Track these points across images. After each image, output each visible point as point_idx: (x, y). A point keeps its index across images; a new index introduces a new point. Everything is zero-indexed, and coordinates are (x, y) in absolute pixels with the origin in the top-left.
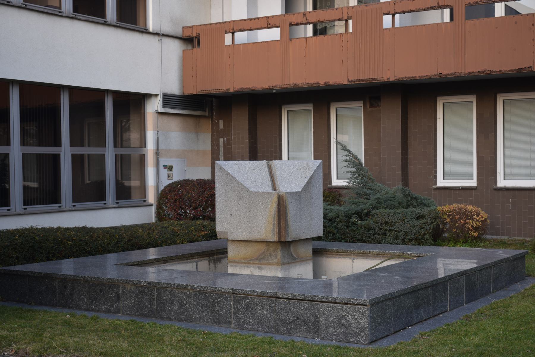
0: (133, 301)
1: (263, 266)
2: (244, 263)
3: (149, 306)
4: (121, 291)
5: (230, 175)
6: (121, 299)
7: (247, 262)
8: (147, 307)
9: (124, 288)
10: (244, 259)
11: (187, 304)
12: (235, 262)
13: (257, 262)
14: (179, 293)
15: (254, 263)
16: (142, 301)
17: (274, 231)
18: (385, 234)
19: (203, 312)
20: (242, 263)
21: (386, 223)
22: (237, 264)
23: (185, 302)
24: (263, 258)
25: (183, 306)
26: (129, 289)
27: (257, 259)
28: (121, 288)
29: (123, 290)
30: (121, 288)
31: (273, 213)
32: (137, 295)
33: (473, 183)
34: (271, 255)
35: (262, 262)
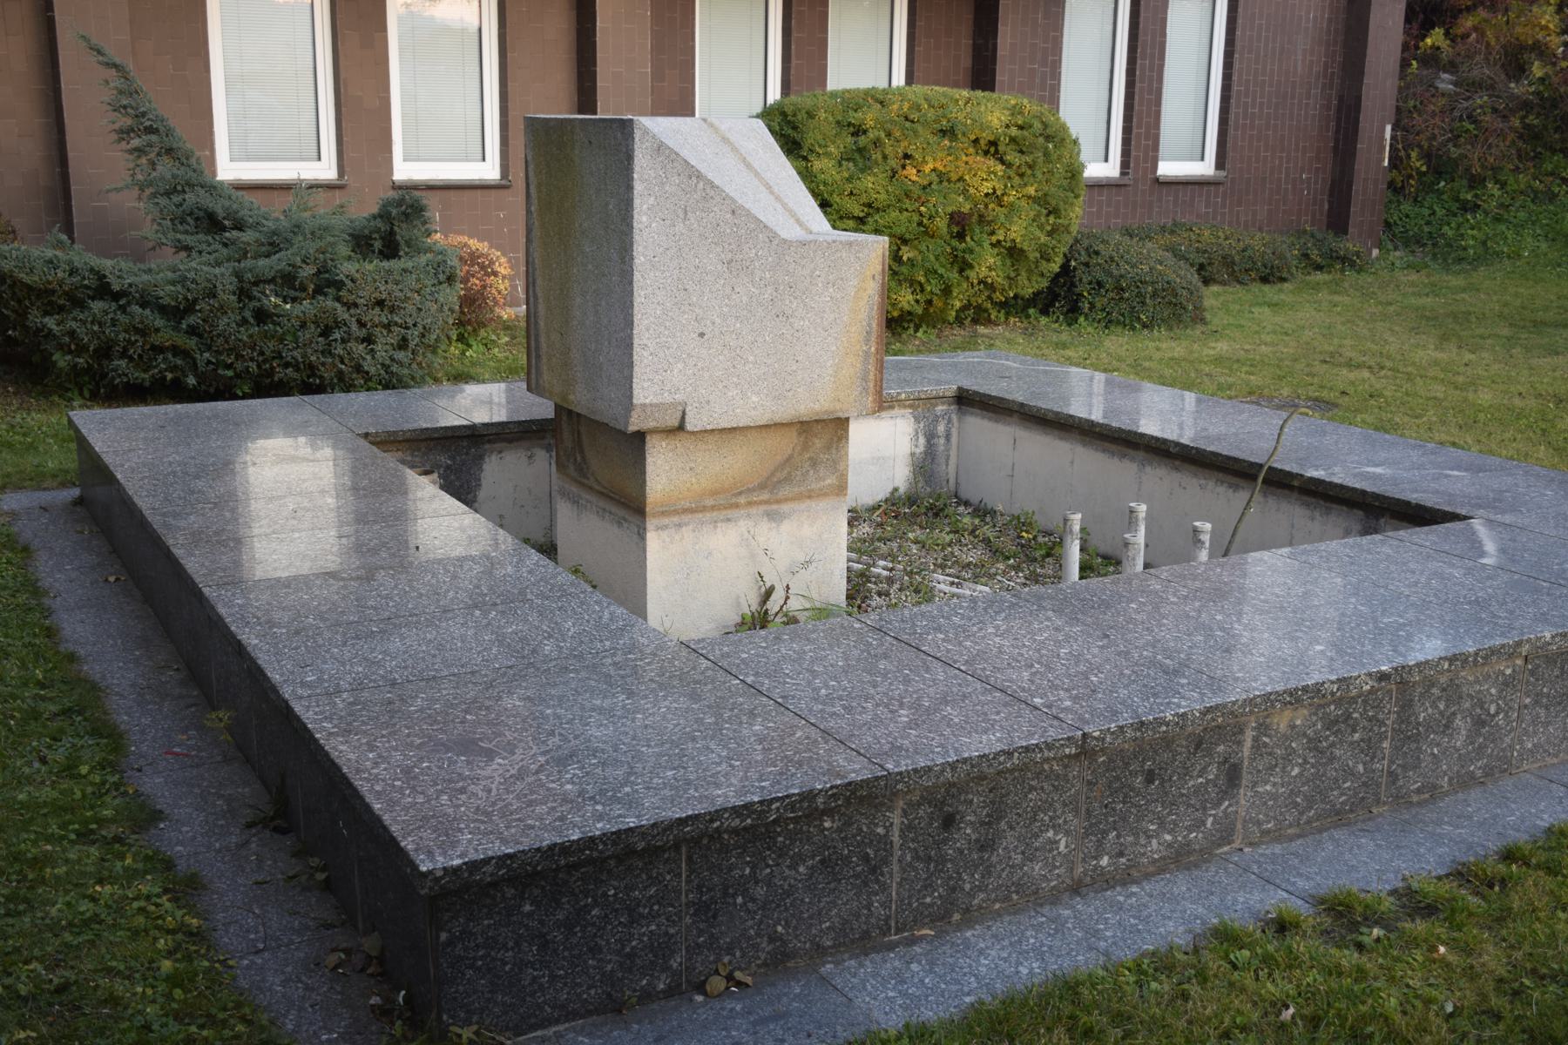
0: (1296, 771)
1: (785, 507)
2: (713, 508)
3: (1361, 768)
4: (1248, 743)
5: (699, 176)
6: (1246, 779)
7: (722, 502)
8: (1352, 773)
9: (1263, 728)
10: (714, 493)
11: (1497, 713)
12: (676, 512)
13: (765, 496)
14: (1477, 681)
15: (750, 504)
16: (1332, 759)
17: (865, 379)
18: (368, 340)
19: (1548, 723)
20: (704, 509)
21: (380, 303)
22: (686, 518)
23: (1493, 710)
24: (788, 479)
25: (1483, 723)
26: (1283, 727)
27: (762, 487)
28: (1249, 734)
29: (1256, 739)
30: (1249, 734)
31: (863, 315)
32: (1314, 744)
33: (326, 170)
34: (814, 463)
35: (785, 491)
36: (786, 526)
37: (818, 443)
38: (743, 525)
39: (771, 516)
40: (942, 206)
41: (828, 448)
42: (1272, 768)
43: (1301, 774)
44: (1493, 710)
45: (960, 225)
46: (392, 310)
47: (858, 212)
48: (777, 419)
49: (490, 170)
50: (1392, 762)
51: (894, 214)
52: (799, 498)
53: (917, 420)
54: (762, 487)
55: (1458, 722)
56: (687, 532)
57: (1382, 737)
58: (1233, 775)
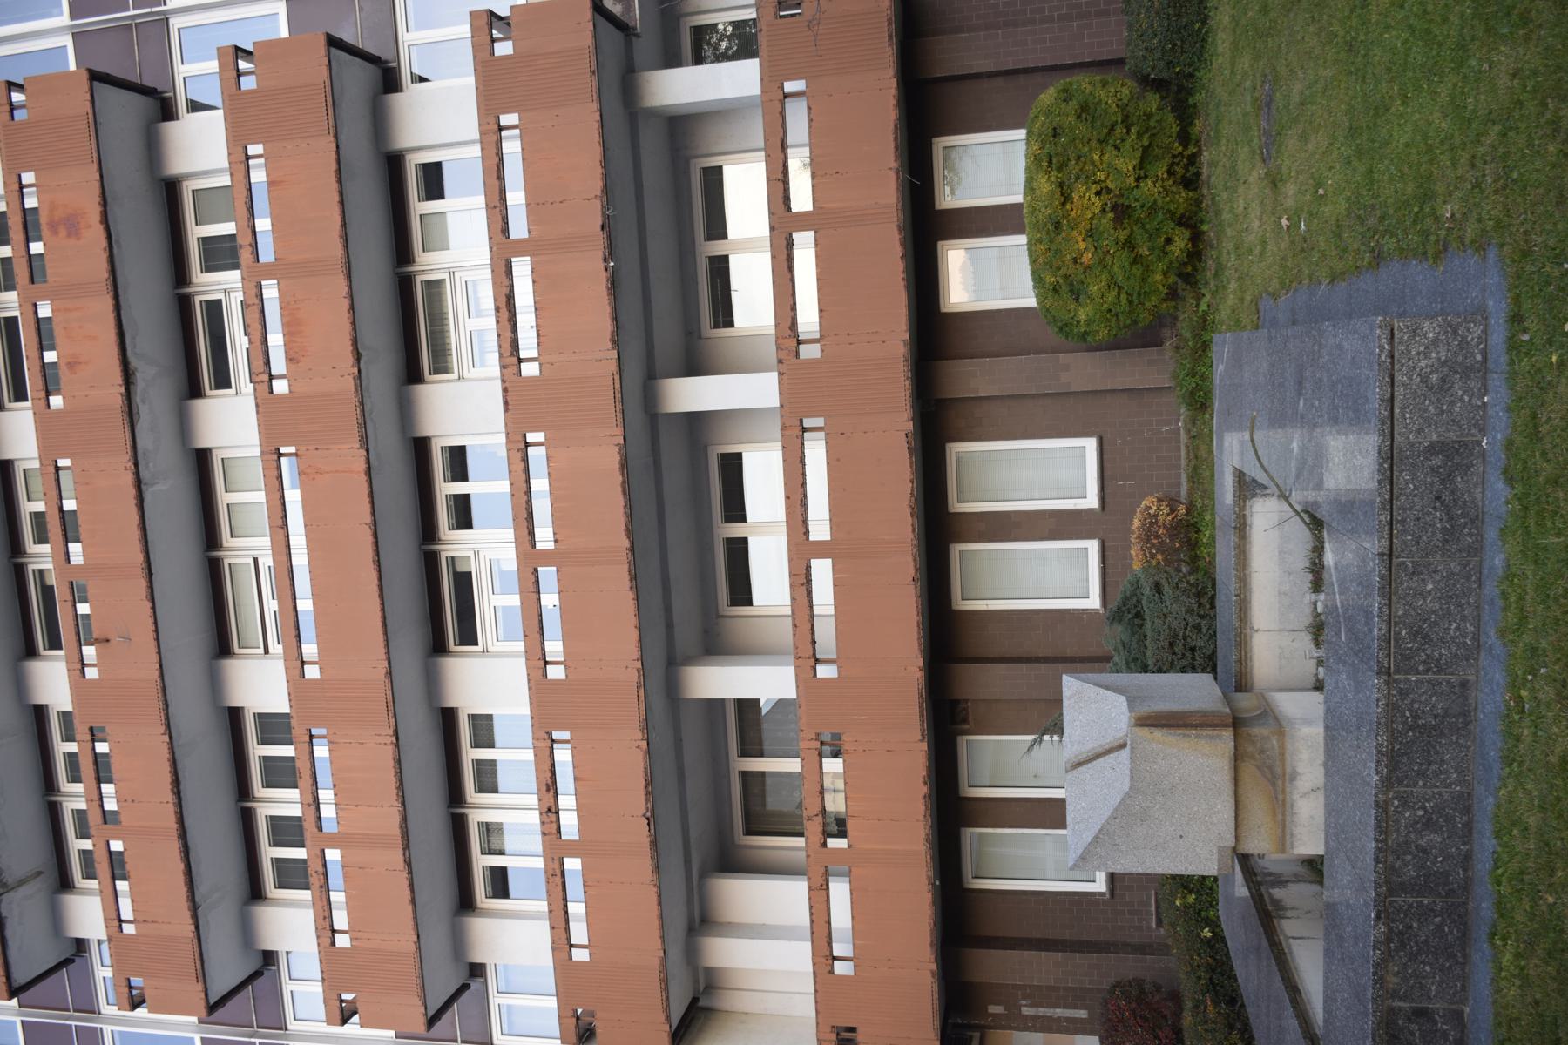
0: (1428, 969)
1: (1288, 770)
2: (1283, 814)
3: (1437, 920)
4: (1402, 1004)
5: (1097, 837)
6: (1424, 1005)
7: (1281, 809)
8: (1439, 927)
9: (1394, 994)
10: (1274, 814)
11: (1424, 808)
12: (1284, 836)
13: (1280, 783)
14: (1398, 830)
15: (1284, 791)
16: (1426, 941)
17: (1211, 737)
18: (1193, 649)
19: (1442, 761)
20: (1284, 821)
21: (1171, 645)
22: (1288, 831)
23: (1421, 813)
24: (1270, 768)
25: (1429, 819)
26: (1396, 980)
27: (1274, 784)
28: (1397, 1004)
29: (1400, 999)
30: (1397, 1004)
31: (1173, 739)
32: (1413, 957)
33: (1093, 546)
34: (1262, 751)
35: (1278, 770)
36: (1299, 770)
37: (1250, 749)
38: (1296, 797)
39: (1293, 778)
40: (1112, 236)
41: (1253, 742)
42: (1422, 987)
43: (1430, 965)
44: (1421, 813)
45: (1121, 212)
46: (1175, 635)
47: (1114, 293)
48: (1231, 793)
49: (1090, 445)
50: (1440, 895)
51: (1116, 269)
52: (1283, 761)
53: (1254, 496)
54: (1274, 784)
55: (1423, 843)
56: (1297, 831)
57: (1420, 904)
58: (1421, 1014)
